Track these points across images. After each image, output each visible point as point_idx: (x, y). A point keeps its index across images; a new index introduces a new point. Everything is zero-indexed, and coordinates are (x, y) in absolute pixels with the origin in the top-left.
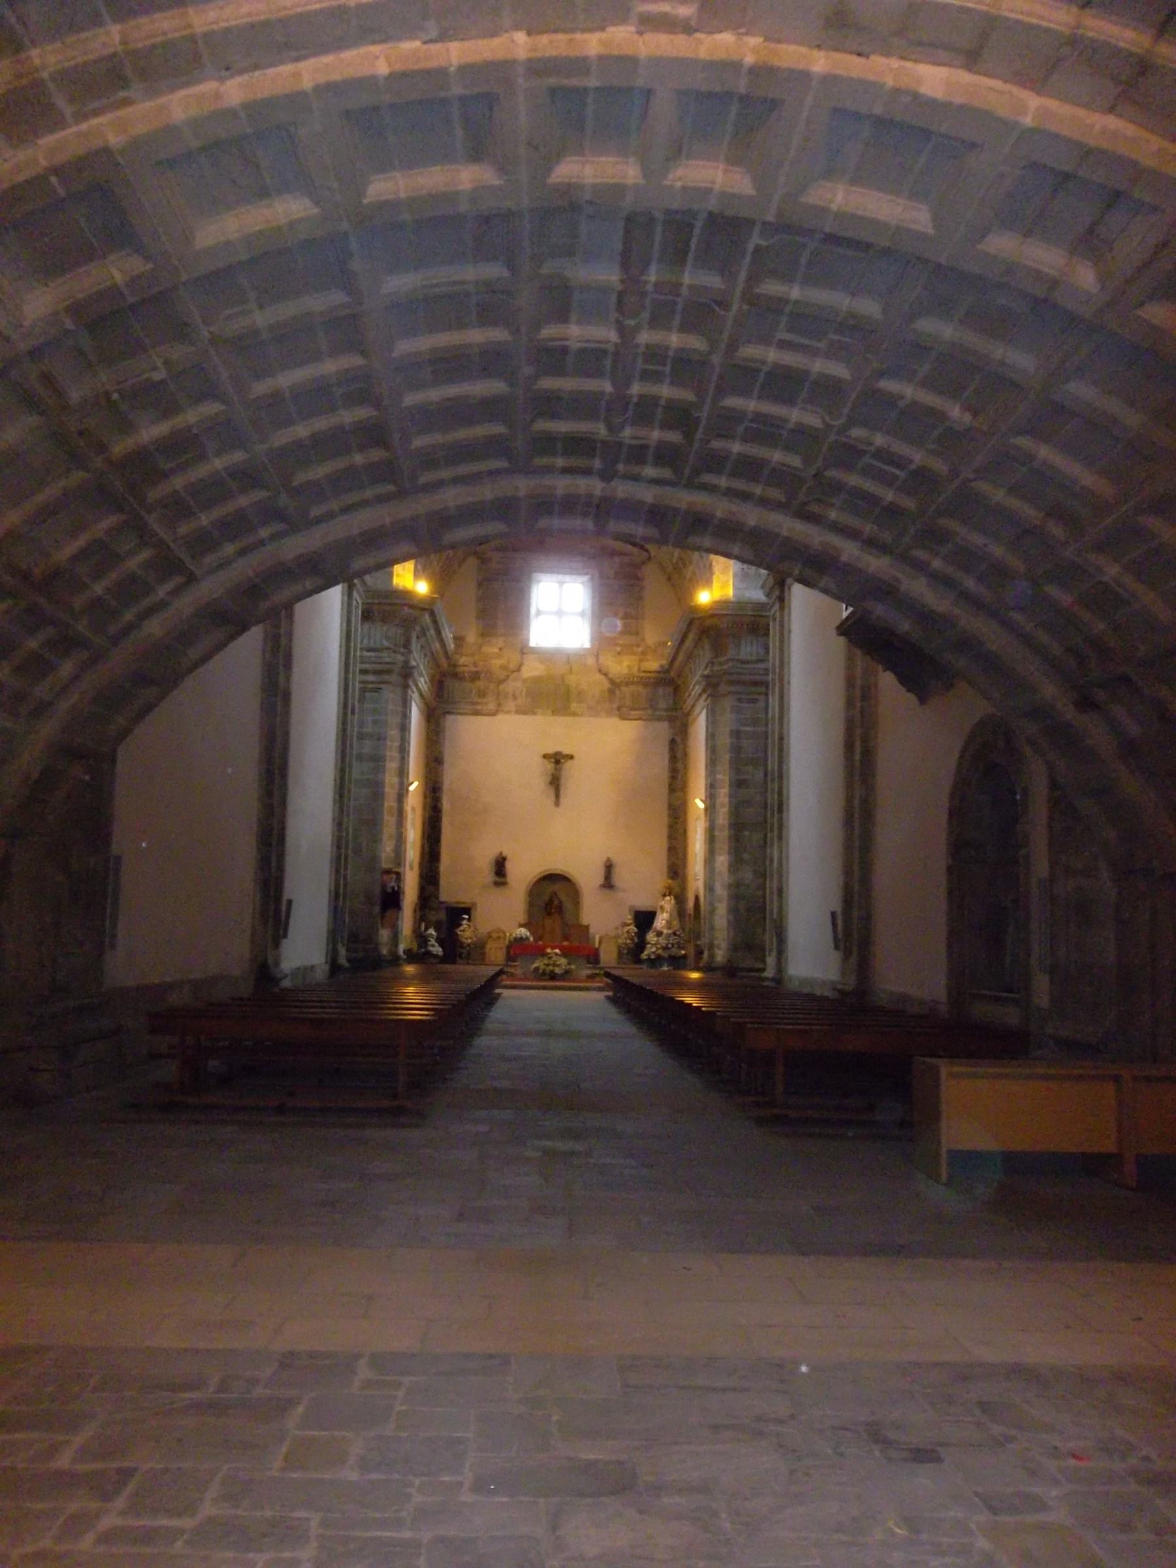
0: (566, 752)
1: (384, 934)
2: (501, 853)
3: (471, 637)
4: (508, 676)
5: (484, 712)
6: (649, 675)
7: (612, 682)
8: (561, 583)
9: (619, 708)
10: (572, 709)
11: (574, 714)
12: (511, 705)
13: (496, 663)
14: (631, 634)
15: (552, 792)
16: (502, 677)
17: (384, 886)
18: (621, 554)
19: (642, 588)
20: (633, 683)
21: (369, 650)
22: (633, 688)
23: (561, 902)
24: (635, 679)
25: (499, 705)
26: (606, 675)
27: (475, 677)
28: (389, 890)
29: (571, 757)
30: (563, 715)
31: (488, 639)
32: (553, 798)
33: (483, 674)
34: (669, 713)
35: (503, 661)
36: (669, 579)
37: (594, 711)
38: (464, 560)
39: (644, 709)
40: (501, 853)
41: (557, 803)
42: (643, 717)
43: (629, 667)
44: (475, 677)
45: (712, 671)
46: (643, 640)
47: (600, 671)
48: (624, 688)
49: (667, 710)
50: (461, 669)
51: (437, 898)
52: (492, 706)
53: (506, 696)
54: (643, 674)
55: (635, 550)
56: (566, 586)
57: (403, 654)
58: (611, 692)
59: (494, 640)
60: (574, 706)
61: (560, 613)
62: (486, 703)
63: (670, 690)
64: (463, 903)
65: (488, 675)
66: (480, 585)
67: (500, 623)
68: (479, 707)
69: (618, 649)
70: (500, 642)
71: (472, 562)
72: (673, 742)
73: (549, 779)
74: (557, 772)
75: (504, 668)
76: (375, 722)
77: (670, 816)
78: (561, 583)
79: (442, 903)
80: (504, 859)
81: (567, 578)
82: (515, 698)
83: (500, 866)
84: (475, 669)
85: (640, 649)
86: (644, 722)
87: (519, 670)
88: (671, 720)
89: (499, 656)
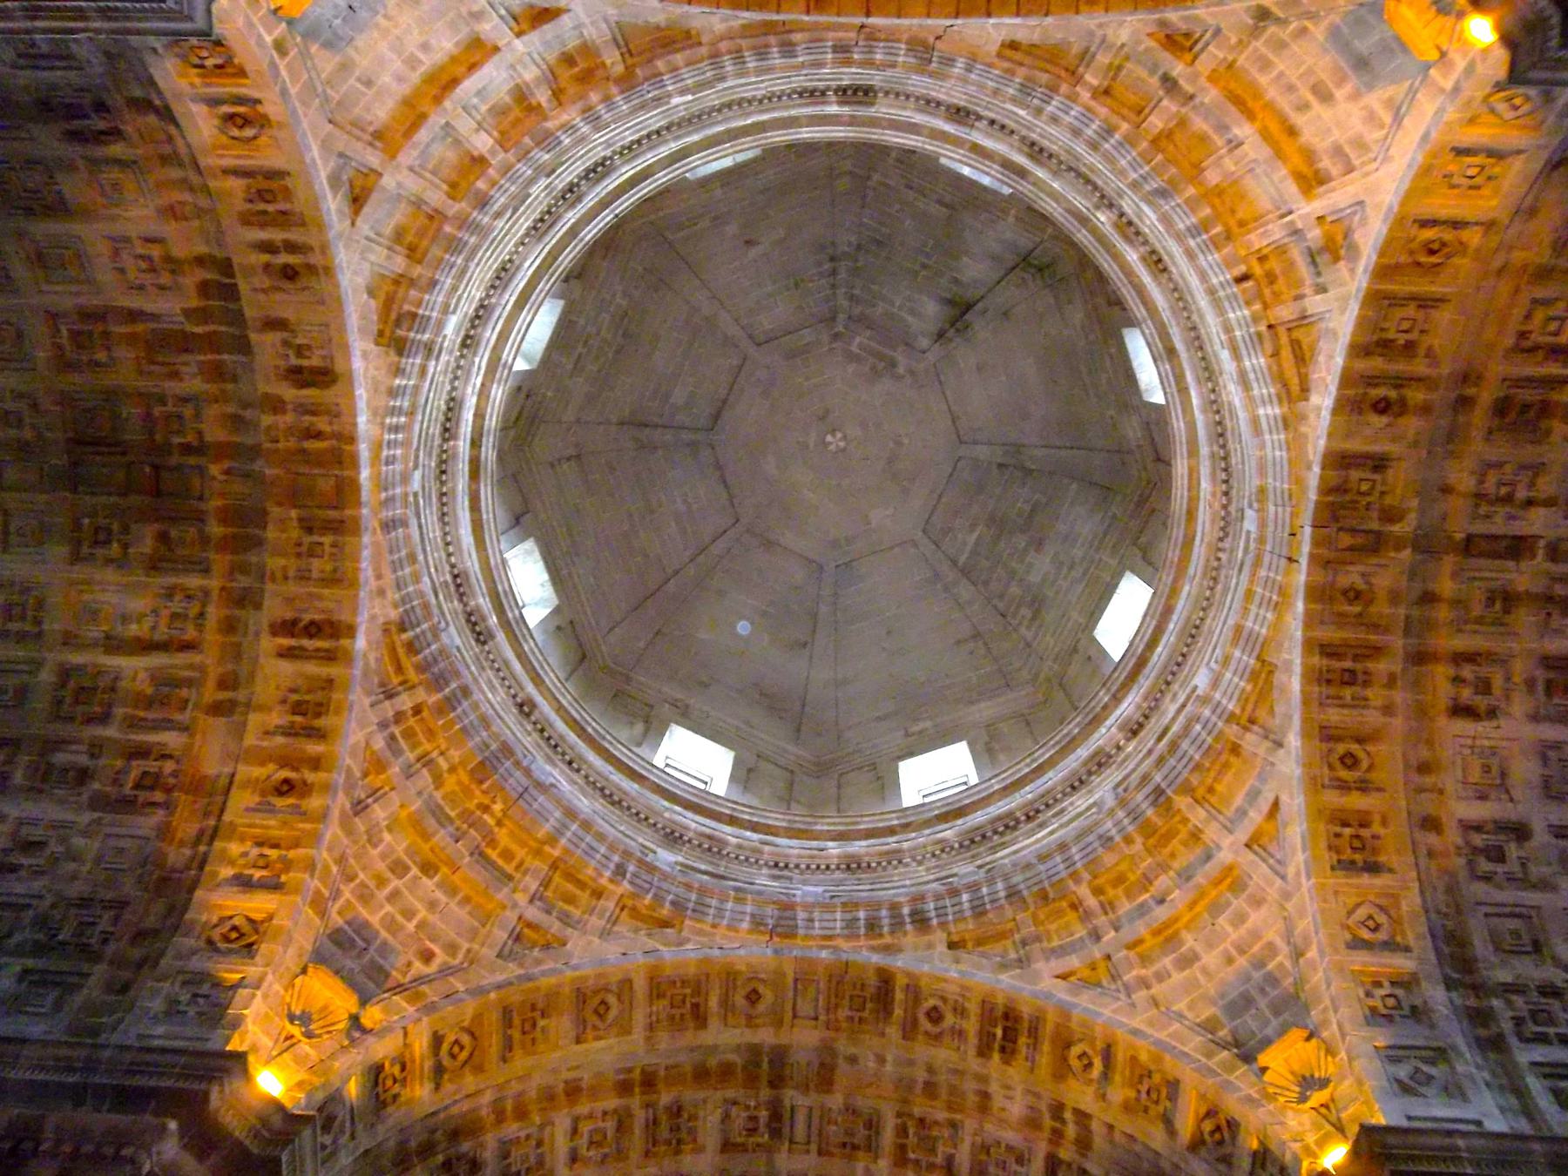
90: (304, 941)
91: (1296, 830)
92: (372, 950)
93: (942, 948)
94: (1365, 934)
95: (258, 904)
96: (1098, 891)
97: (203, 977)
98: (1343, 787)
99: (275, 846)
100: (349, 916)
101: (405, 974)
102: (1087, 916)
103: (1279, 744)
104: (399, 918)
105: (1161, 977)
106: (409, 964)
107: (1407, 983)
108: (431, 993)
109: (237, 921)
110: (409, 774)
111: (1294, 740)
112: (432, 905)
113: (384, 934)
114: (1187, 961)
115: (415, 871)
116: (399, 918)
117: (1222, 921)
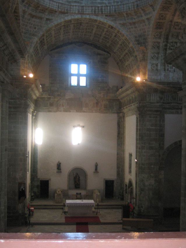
1: (20, 206)
2: (59, 162)
17: (19, 188)
18: (100, 54)
21: (11, 99)
28: (21, 190)
36: (118, 63)
40: (59, 162)
51: (37, 177)
55: (106, 53)
80: (60, 164)
82: (63, 106)
83: (59, 166)
91: (153, 22)
93: (105, 16)
94: (156, 36)
96: (127, 14)
98: (160, 19)
102: (124, 17)
103: (154, 11)
104: (31, 26)
105: (132, 28)
107: (159, 43)
110: (28, 9)
111: (156, 12)
112: (34, 21)
113: (30, 29)
114: (135, 27)
115: (31, 19)
116: (31, 26)
117: (141, 25)
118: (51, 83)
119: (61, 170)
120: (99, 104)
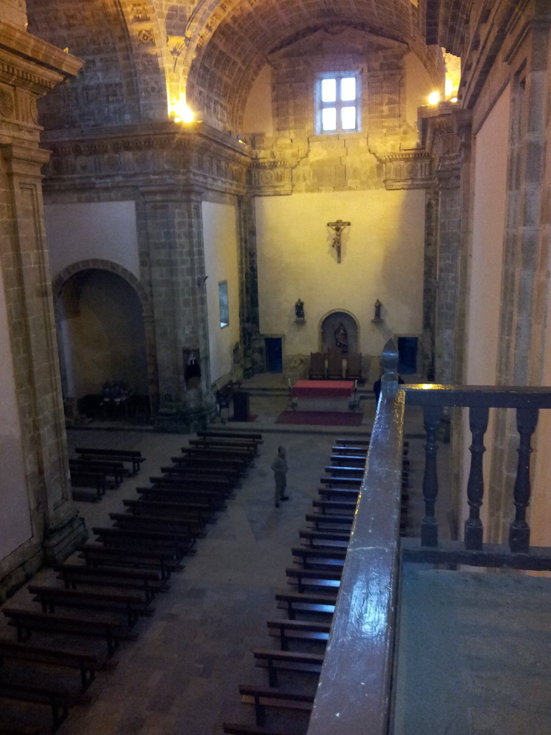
0: (344, 220)
1: (191, 394)
2: (299, 300)
3: (270, 133)
4: (299, 162)
5: (282, 193)
6: (409, 152)
7: (380, 160)
8: (339, 79)
9: (385, 181)
10: (349, 185)
11: (351, 189)
12: (302, 185)
13: (288, 152)
14: (394, 116)
15: (335, 252)
16: (294, 164)
17: (186, 361)
19: (403, 77)
20: (396, 159)
22: (395, 163)
23: (345, 331)
24: (397, 157)
25: (293, 186)
26: (374, 154)
27: (274, 165)
28: (189, 363)
29: (349, 224)
30: (342, 190)
31: (282, 132)
32: (336, 255)
33: (279, 163)
34: (425, 182)
35: (295, 150)
37: (365, 185)
38: (259, 67)
39: (405, 180)
40: (299, 300)
41: (339, 262)
42: (405, 187)
43: (393, 146)
44: (274, 165)
45: (443, 166)
46: (404, 121)
47: (370, 151)
48: (389, 164)
49: (422, 180)
50: (261, 161)
51: (259, 333)
52: (288, 188)
53: (298, 178)
54: (403, 152)
55: (396, 44)
56: (344, 81)
57: (184, 174)
58: (379, 168)
59: (287, 133)
60: (350, 182)
61: (338, 104)
62: (283, 186)
63: (427, 162)
64: (276, 335)
65: (282, 163)
66: (274, 88)
67: (291, 118)
68: (278, 189)
69: (385, 131)
70: (292, 134)
71: (266, 70)
72: (429, 206)
73: (331, 242)
74: (338, 237)
75: (295, 155)
76: (168, 234)
77: (426, 265)
78: (339, 79)
79: (262, 335)
80: (302, 304)
81: (342, 74)
82: (305, 179)
83: (300, 308)
84: (272, 160)
85: (402, 129)
86: (406, 190)
87: (307, 156)
88: (427, 187)
89: (291, 147)
90: (163, 29)
92: (178, 12)
95: (146, 26)
97: (146, 55)
99: (139, 5)
100: (168, 8)
101: (190, 12)
106: (190, 8)
108: (199, 15)
109: (144, 32)
118: (278, 130)
119: (306, 318)
120: (384, 168)
